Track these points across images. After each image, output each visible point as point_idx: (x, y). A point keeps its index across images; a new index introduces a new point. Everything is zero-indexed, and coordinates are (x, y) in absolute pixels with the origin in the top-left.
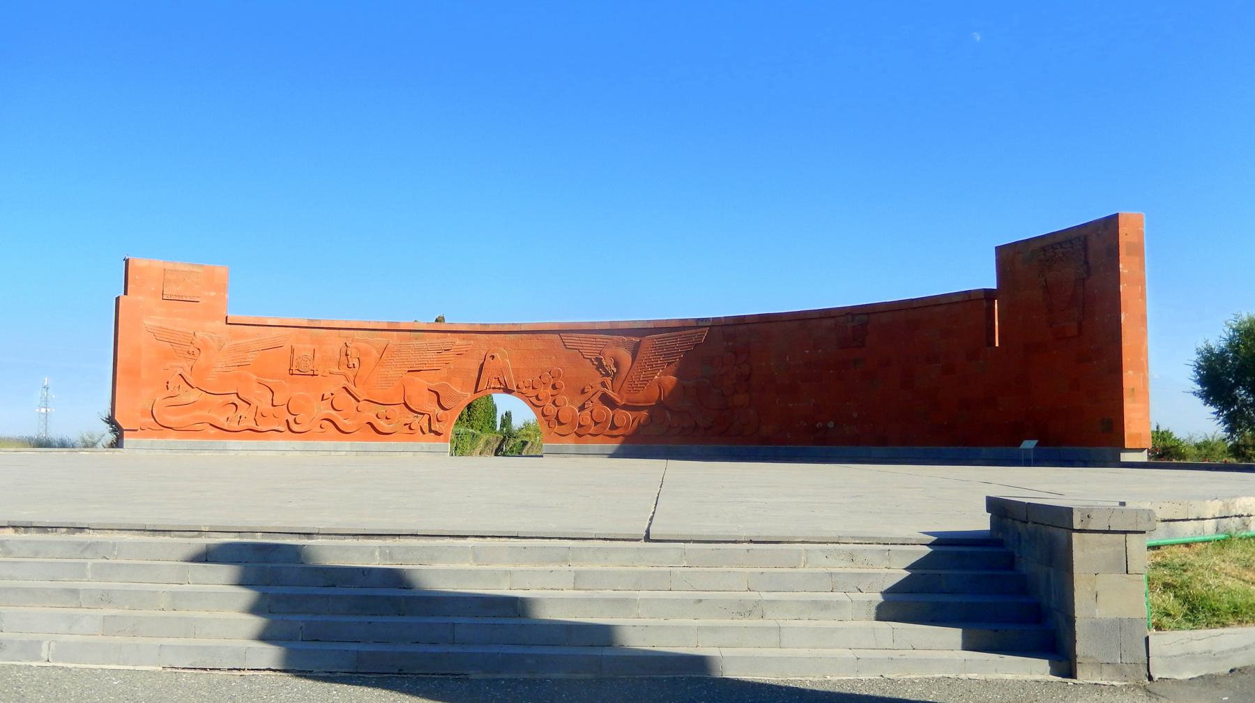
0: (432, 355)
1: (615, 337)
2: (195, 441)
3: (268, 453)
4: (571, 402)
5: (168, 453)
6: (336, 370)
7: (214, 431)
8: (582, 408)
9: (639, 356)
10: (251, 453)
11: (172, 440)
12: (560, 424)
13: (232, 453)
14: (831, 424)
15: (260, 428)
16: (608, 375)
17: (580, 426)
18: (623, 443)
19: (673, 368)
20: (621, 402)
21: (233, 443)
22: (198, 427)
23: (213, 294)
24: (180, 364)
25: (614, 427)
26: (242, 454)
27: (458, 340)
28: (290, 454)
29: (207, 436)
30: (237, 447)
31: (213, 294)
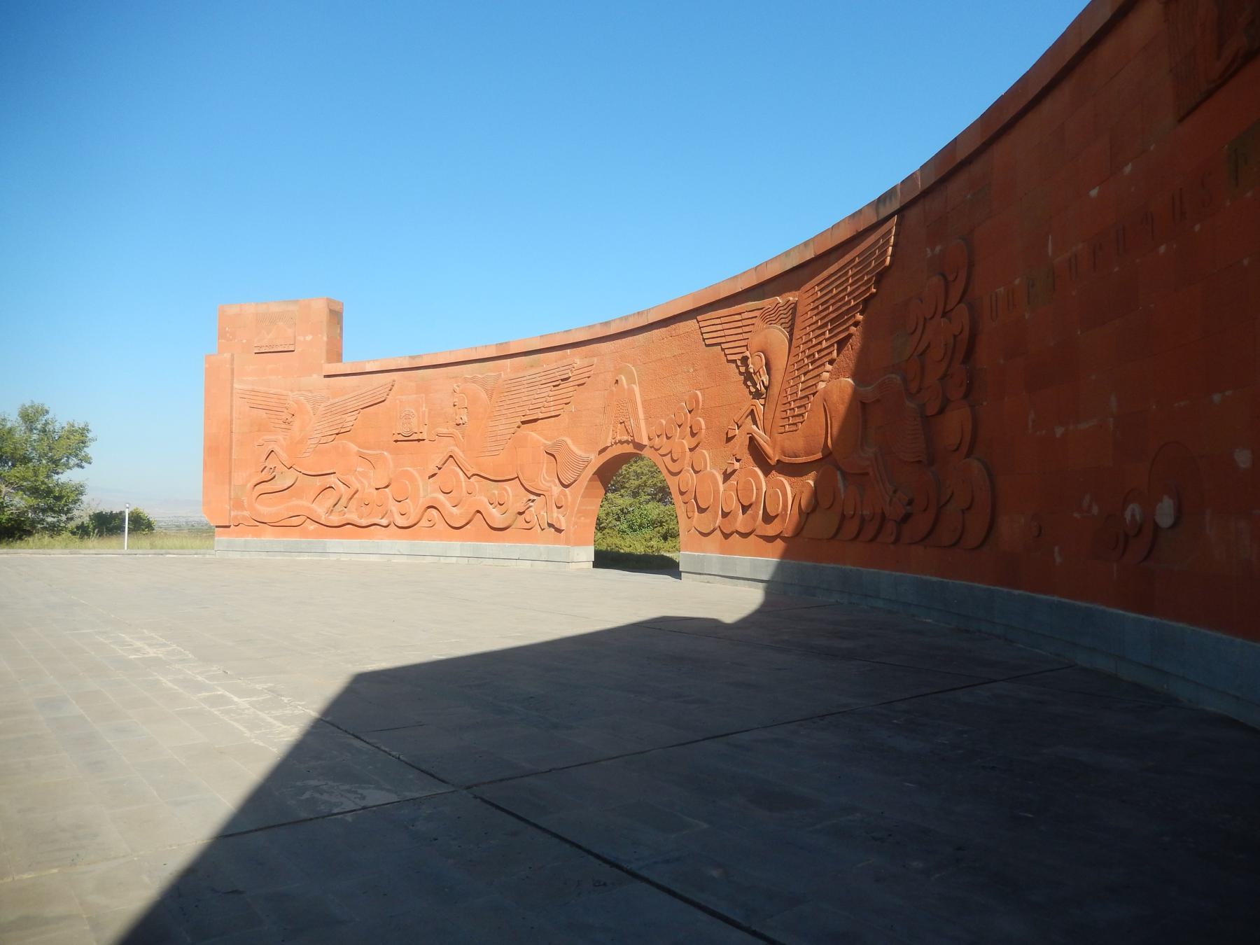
0: (547, 391)
1: (767, 303)
2: (293, 539)
3: (373, 558)
4: (714, 465)
5: (264, 556)
6: (445, 431)
7: (312, 527)
8: (727, 476)
9: (797, 334)
10: (355, 558)
11: (269, 538)
12: (701, 510)
13: (333, 558)
14: (1165, 512)
15: (364, 522)
16: (757, 395)
17: (725, 515)
18: (785, 555)
19: (849, 355)
20: (774, 455)
21: (335, 544)
22: (295, 521)
23: (309, 338)
24: (273, 437)
25: (768, 519)
26: (344, 558)
27: (576, 358)
28: (396, 560)
29: (306, 534)
30: (341, 548)
31: (309, 338)
